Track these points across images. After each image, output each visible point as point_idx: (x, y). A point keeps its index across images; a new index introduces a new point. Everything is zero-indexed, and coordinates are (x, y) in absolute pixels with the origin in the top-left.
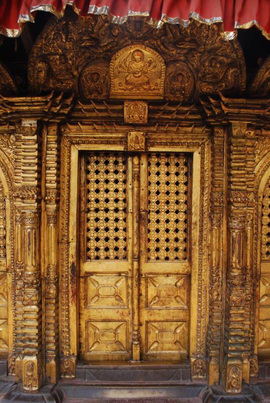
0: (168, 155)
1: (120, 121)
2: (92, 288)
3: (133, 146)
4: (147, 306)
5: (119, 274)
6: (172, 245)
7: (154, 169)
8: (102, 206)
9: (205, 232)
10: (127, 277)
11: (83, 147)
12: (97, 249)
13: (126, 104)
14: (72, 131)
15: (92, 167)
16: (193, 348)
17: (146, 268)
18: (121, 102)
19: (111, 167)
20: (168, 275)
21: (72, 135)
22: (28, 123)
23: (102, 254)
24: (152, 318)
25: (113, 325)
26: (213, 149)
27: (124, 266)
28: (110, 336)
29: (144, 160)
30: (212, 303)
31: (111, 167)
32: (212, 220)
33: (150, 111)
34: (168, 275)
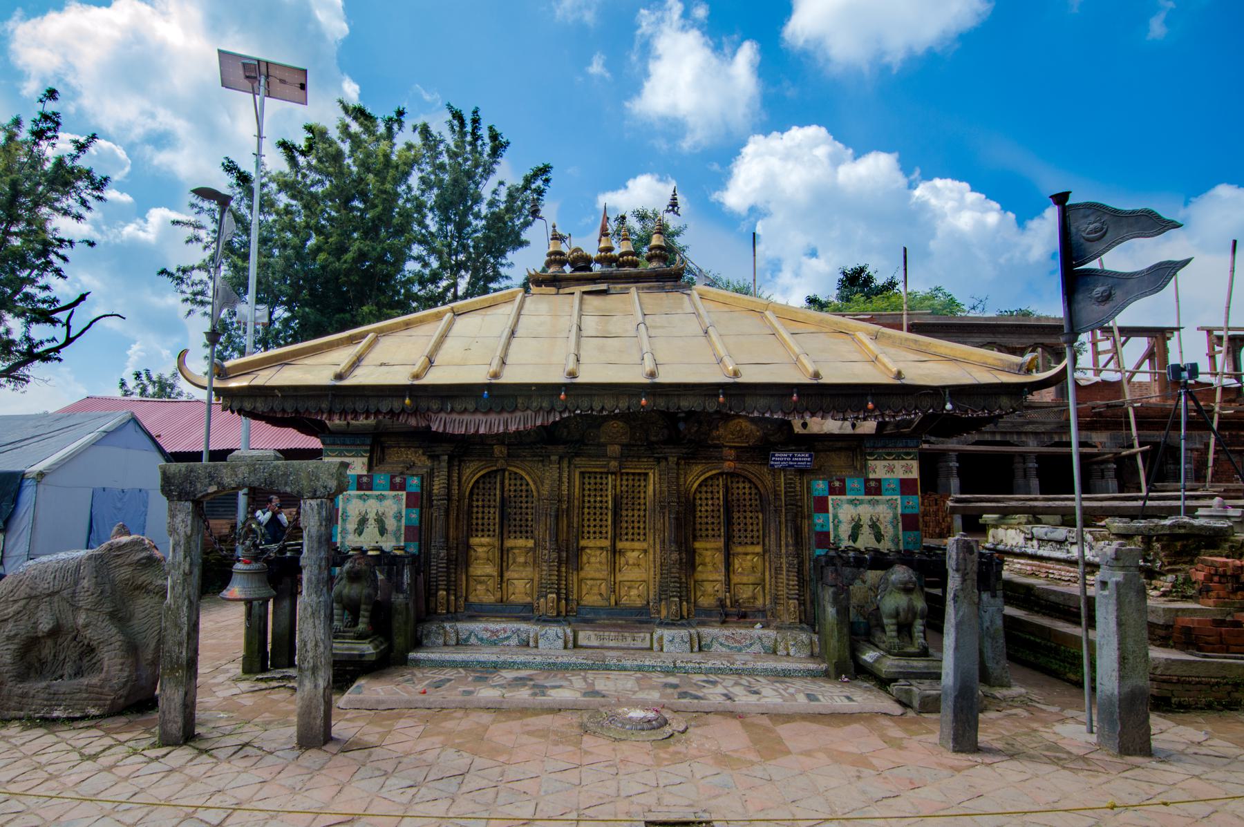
0: (634, 474)
1: (605, 456)
2: (585, 558)
3: (612, 469)
5: (602, 548)
6: (636, 531)
7: (625, 483)
14: (577, 461)
15: (587, 480)
16: (651, 596)
17: (620, 545)
18: (604, 445)
19: (598, 480)
22: (553, 458)
23: (592, 536)
28: (595, 590)
31: (598, 480)
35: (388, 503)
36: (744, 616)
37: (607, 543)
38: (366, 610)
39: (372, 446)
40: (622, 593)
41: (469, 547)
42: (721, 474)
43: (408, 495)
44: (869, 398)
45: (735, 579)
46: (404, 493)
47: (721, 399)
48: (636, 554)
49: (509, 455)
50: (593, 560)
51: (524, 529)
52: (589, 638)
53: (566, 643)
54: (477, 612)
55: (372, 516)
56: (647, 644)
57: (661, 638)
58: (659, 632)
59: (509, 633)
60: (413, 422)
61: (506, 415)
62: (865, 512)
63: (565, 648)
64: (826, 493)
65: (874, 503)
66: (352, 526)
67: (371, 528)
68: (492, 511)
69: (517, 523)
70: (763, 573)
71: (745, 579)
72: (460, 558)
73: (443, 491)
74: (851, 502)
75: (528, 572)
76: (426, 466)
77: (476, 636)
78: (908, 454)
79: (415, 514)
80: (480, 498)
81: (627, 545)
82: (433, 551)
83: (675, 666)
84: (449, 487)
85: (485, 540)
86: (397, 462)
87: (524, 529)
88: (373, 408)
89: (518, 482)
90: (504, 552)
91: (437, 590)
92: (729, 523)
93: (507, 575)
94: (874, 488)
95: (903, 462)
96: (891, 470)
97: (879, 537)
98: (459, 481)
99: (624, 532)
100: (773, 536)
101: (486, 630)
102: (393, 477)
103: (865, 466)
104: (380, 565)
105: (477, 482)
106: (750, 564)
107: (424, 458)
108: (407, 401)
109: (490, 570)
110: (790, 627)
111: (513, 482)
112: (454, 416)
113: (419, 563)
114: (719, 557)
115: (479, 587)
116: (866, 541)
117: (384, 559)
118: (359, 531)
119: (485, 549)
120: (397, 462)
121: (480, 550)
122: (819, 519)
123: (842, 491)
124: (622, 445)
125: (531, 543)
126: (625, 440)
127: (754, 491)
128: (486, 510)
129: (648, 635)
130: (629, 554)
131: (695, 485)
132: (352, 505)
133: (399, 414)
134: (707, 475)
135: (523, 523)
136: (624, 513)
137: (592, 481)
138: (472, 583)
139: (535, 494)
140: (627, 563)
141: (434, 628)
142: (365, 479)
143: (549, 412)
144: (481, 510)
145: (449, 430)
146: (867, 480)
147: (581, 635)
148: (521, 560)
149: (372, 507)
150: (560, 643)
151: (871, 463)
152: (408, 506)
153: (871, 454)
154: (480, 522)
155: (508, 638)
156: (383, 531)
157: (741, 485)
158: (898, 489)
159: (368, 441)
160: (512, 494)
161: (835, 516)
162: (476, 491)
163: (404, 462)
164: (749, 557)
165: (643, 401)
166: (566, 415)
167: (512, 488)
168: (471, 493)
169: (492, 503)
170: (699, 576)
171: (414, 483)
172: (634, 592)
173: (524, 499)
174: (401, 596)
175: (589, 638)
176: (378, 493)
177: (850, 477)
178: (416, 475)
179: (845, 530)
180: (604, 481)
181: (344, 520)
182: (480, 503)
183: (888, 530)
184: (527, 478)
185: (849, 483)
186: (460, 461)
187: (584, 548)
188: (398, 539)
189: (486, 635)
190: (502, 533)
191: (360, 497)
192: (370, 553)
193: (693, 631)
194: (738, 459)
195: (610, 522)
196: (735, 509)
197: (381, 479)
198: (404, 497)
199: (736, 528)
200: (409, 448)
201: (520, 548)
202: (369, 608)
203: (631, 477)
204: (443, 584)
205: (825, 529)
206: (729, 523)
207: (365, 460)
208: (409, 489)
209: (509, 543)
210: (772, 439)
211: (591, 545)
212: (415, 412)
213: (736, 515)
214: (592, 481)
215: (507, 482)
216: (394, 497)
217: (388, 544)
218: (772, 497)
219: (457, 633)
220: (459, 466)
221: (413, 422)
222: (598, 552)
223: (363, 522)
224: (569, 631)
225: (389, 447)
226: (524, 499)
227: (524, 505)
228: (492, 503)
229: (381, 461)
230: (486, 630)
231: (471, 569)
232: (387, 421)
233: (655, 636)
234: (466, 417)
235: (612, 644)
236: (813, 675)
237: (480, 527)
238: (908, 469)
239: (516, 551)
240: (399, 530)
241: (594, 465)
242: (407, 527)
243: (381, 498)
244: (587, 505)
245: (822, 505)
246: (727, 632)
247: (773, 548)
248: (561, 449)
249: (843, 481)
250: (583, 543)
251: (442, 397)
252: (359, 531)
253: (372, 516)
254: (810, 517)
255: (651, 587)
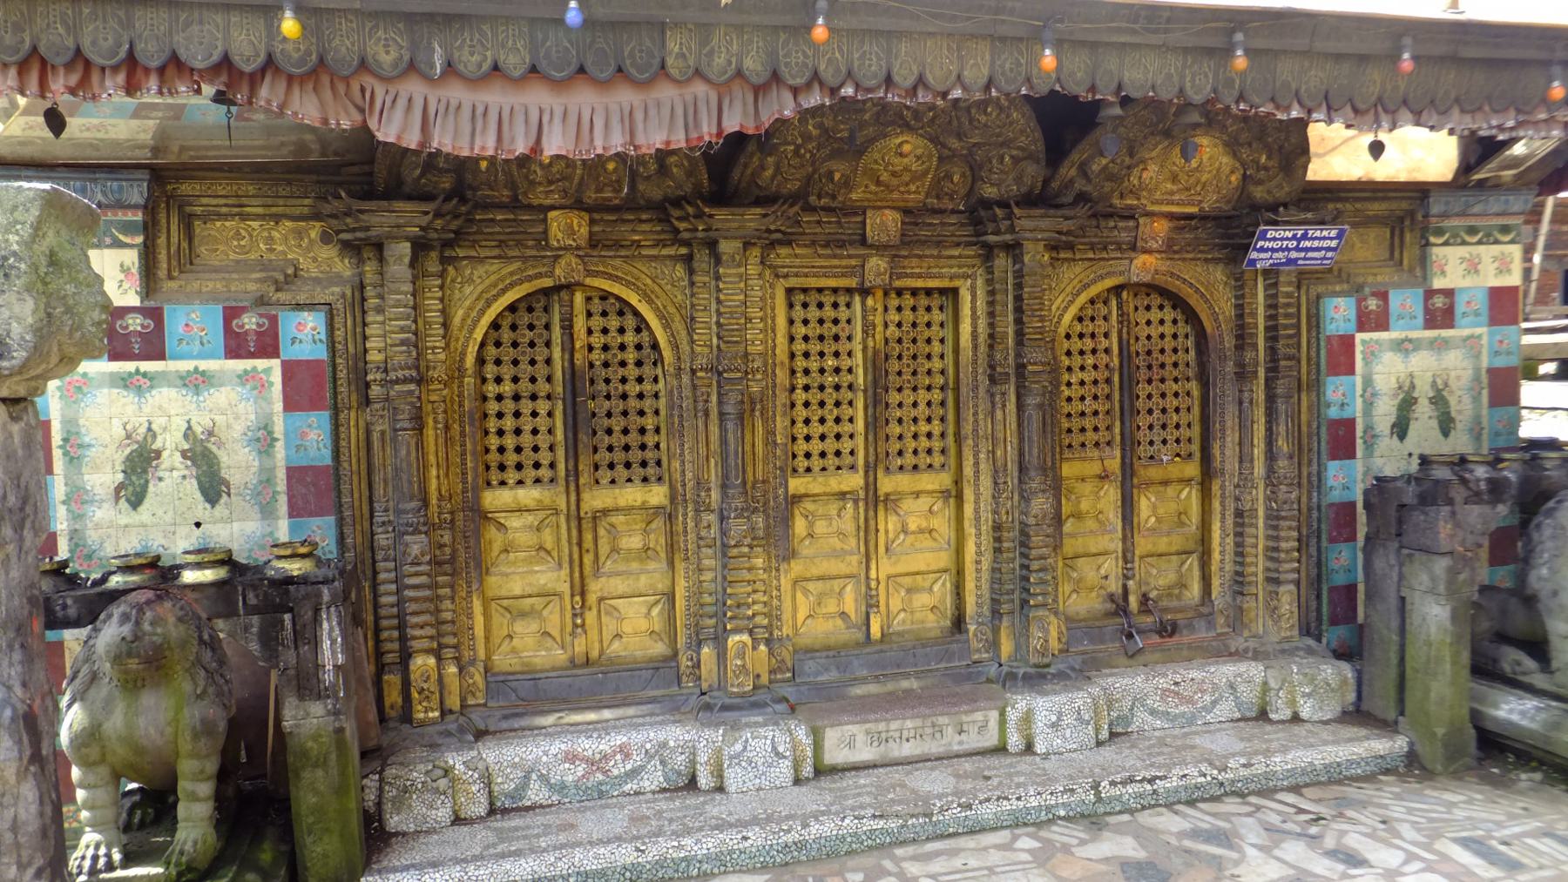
0: (914, 292)
2: (800, 526)
4: (887, 550)
5: (842, 495)
6: (924, 443)
8: (815, 380)
9: (981, 416)
10: (856, 502)
11: (793, 282)
12: (808, 455)
13: (869, 213)
15: (799, 313)
17: (886, 484)
19: (829, 312)
20: (917, 494)
21: (779, 262)
24: (901, 569)
25: (836, 584)
26: (989, 282)
27: (855, 481)
29: (857, 299)
30: (997, 527)
32: (992, 395)
33: (903, 223)
34: (917, 494)
35: (221, 397)
36: (1168, 630)
37: (855, 481)
38: (198, 777)
39: (150, 208)
40: (896, 603)
41: (481, 516)
42: (1117, 290)
43: (289, 369)
44: (1557, 70)
45: (1142, 545)
46: (275, 363)
47: (1240, 61)
48: (924, 503)
49: (593, 243)
50: (821, 527)
51: (636, 455)
52: (851, 745)
53: (797, 766)
54: (521, 700)
55: (170, 442)
56: (991, 740)
57: (1027, 719)
58: (1020, 703)
59: (637, 759)
60: (307, 109)
61: (625, 96)
62: (1422, 365)
63: (797, 781)
64: (1352, 325)
65: (1439, 346)
66: (103, 477)
67: (174, 481)
68: (543, 407)
69: (617, 439)
70: (1205, 526)
71: (1163, 544)
72: (462, 547)
73: (400, 357)
74: (1403, 347)
75: (653, 575)
76: (337, 279)
77: (544, 779)
78: (1505, 229)
79: (315, 430)
80: (507, 371)
81: (903, 482)
82: (382, 539)
83: (1099, 799)
84: (416, 342)
85: (529, 495)
86: (241, 267)
87: (636, 455)
88: (151, 54)
89: (614, 323)
90: (582, 523)
91: (406, 656)
92: (1128, 411)
93: (595, 588)
94: (1441, 313)
95: (1496, 249)
96: (1473, 267)
97: (1446, 425)
98: (445, 325)
99: (895, 446)
100: (1232, 438)
101: (571, 758)
102: (231, 314)
103: (1423, 260)
104: (230, 613)
105: (495, 325)
106: (1173, 506)
107: (328, 253)
108: (289, 26)
109: (551, 577)
110: (1287, 653)
111: (597, 322)
112: (456, 93)
113: (355, 580)
114: (1111, 495)
115: (519, 627)
116: (1424, 435)
117: (239, 581)
118: (133, 491)
119: (530, 519)
120: (241, 267)
121: (514, 522)
122: (1335, 388)
123: (1382, 323)
124: (906, 212)
125: (657, 495)
126: (915, 195)
127: (1183, 329)
128: (526, 406)
129: (994, 715)
130: (907, 505)
131: (1068, 318)
132: (96, 409)
133: (255, 79)
134: (1093, 291)
135: (633, 439)
136: (894, 398)
137: (813, 313)
138: (500, 622)
139: (667, 354)
140: (905, 530)
141: (418, 775)
142: (135, 323)
143: (759, 90)
144: (509, 406)
145: (445, 140)
146: (1430, 293)
147: (831, 736)
148: (634, 542)
149: (169, 412)
150: (784, 770)
151: (1438, 253)
152: (290, 405)
153: (1439, 232)
154: (510, 441)
155: (634, 773)
156: (213, 488)
157: (1155, 315)
158: (1485, 318)
159: (137, 192)
160: (598, 357)
161: (1368, 381)
162: (492, 351)
163: (263, 265)
164: (1171, 491)
165: (1048, 59)
166: (814, 99)
167: (597, 340)
168: (481, 361)
169: (542, 387)
170: (1069, 546)
171: (305, 334)
172: (923, 600)
173: (632, 372)
174: (317, 709)
175: (851, 745)
176: (185, 366)
177: (1399, 286)
178: (310, 306)
179: (1385, 410)
180: (843, 314)
181: (73, 460)
182: (507, 388)
183: (1462, 407)
184: (644, 309)
185: (1396, 299)
186: (444, 261)
187: (797, 499)
188: (267, 512)
189: (572, 774)
190: (574, 473)
191: (124, 382)
192: (189, 577)
193: (1096, 691)
194: (1169, 249)
195: (860, 424)
196: (1143, 374)
197: (193, 321)
198: (277, 377)
199: (1143, 421)
200: (277, 218)
201: (628, 510)
202: (212, 766)
203: (909, 301)
204: (420, 637)
205: (1346, 414)
206: (1128, 411)
207: (131, 257)
208: (290, 352)
209: (595, 499)
210: (1259, 193)
211: (815, 488)
212: (317, 71)
213: (1143, 389)
214: (813, 313)
215: (580, 324)
216: (245, 378)
217: (242, 530)
218: (1229, 342)
219: (487, 780)
220: (442, 275)
221: (307, 109)
222: (833, 509)
223: (141, 463)
224: (802, 734)
225: (206, 218)
226: (632, 372)
227: (633, 388)
228: (542, 387)
229: (186, 261)
230: (571, 758)
231: (492, 581)
232: (199, 105)
233: (1013, 715)
234: (495, 98)
235: (908, 750)
236: (1382, 770)
237: (511, 458)
238: (1503, 269)
239: (618, 520)
240: (267, 481)
241: (825, 271)
242: (294, 473)
243: (197, 382)
244: (801, 381)
245: (1342, 357)
246: (1163, 683)
247: (1232, 465)
248: (752, 219)
249: (1383, 296)
250: (796, 485)
251: (411, 19)
252: (133, 491)
253: (170, 442)
254: (1316, 386)
255: (970, 585)
